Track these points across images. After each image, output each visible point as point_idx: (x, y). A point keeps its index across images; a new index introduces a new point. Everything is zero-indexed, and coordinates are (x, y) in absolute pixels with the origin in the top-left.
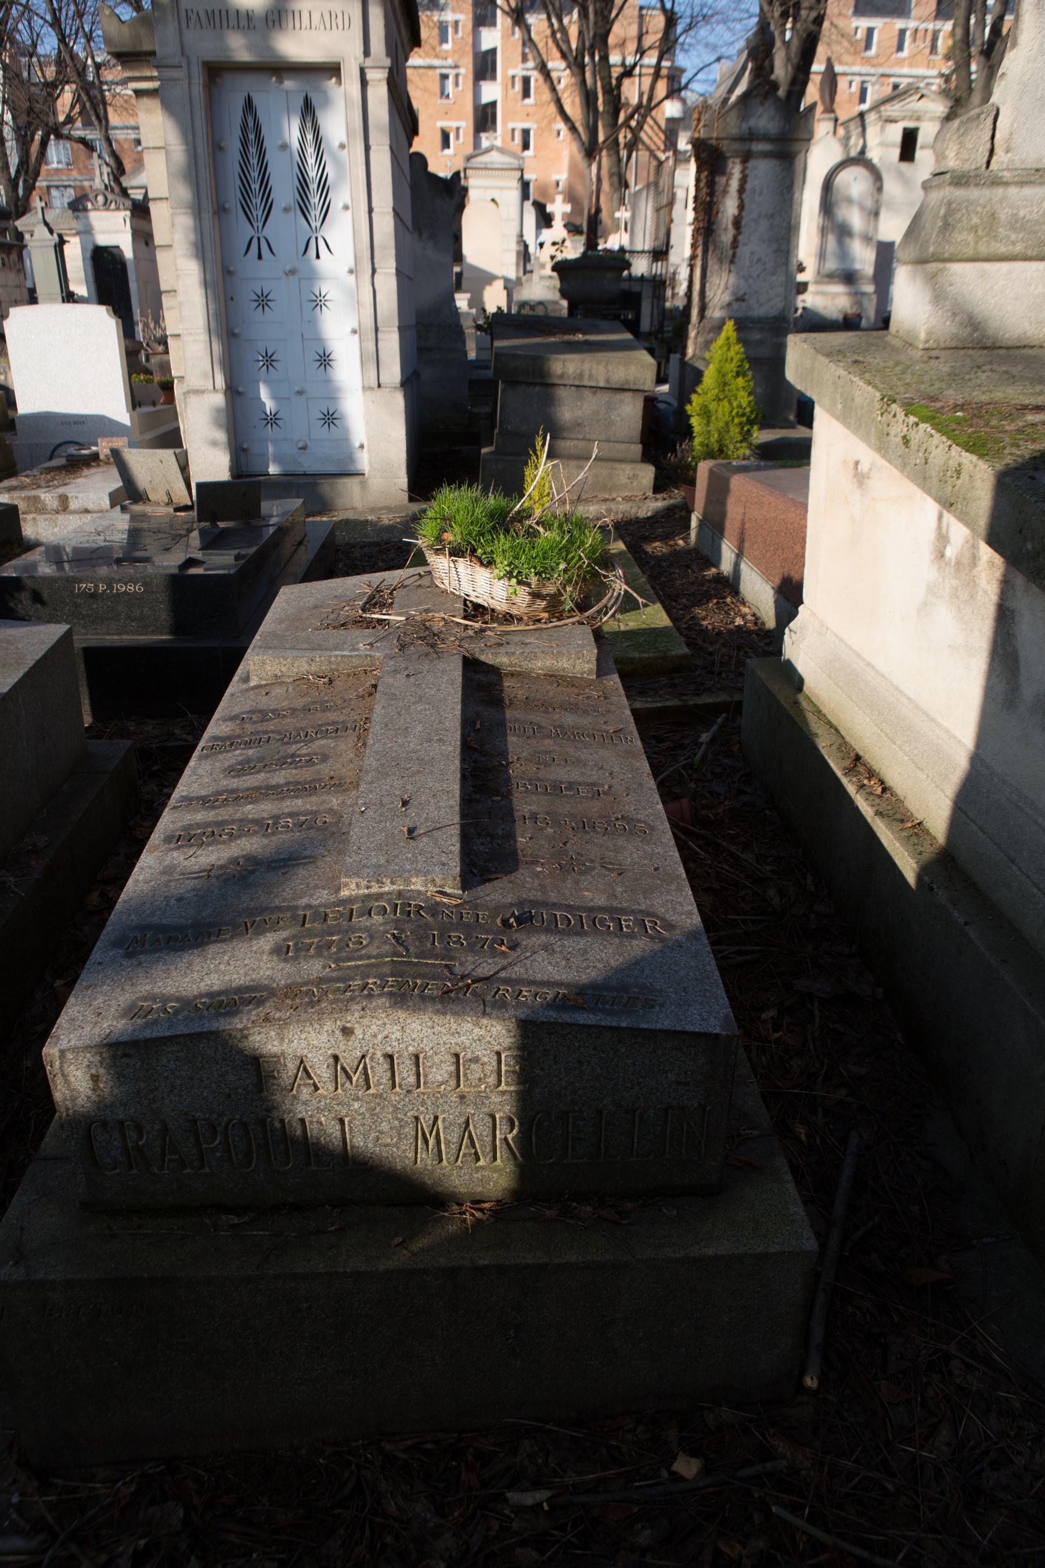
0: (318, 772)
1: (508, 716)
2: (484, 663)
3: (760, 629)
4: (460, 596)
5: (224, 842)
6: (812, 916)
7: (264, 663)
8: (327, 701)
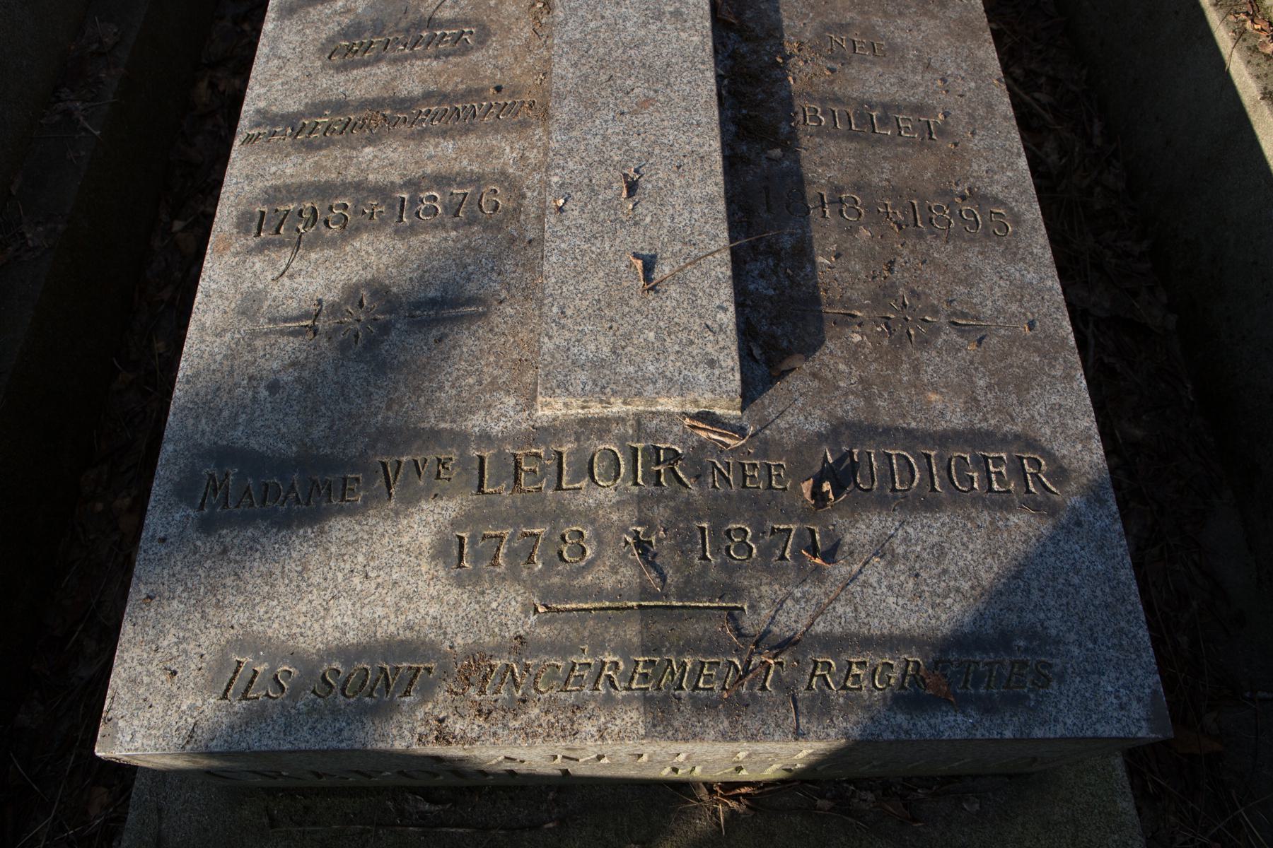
0: (474, 71)
5: (332, 243)
6: (1098, 189)
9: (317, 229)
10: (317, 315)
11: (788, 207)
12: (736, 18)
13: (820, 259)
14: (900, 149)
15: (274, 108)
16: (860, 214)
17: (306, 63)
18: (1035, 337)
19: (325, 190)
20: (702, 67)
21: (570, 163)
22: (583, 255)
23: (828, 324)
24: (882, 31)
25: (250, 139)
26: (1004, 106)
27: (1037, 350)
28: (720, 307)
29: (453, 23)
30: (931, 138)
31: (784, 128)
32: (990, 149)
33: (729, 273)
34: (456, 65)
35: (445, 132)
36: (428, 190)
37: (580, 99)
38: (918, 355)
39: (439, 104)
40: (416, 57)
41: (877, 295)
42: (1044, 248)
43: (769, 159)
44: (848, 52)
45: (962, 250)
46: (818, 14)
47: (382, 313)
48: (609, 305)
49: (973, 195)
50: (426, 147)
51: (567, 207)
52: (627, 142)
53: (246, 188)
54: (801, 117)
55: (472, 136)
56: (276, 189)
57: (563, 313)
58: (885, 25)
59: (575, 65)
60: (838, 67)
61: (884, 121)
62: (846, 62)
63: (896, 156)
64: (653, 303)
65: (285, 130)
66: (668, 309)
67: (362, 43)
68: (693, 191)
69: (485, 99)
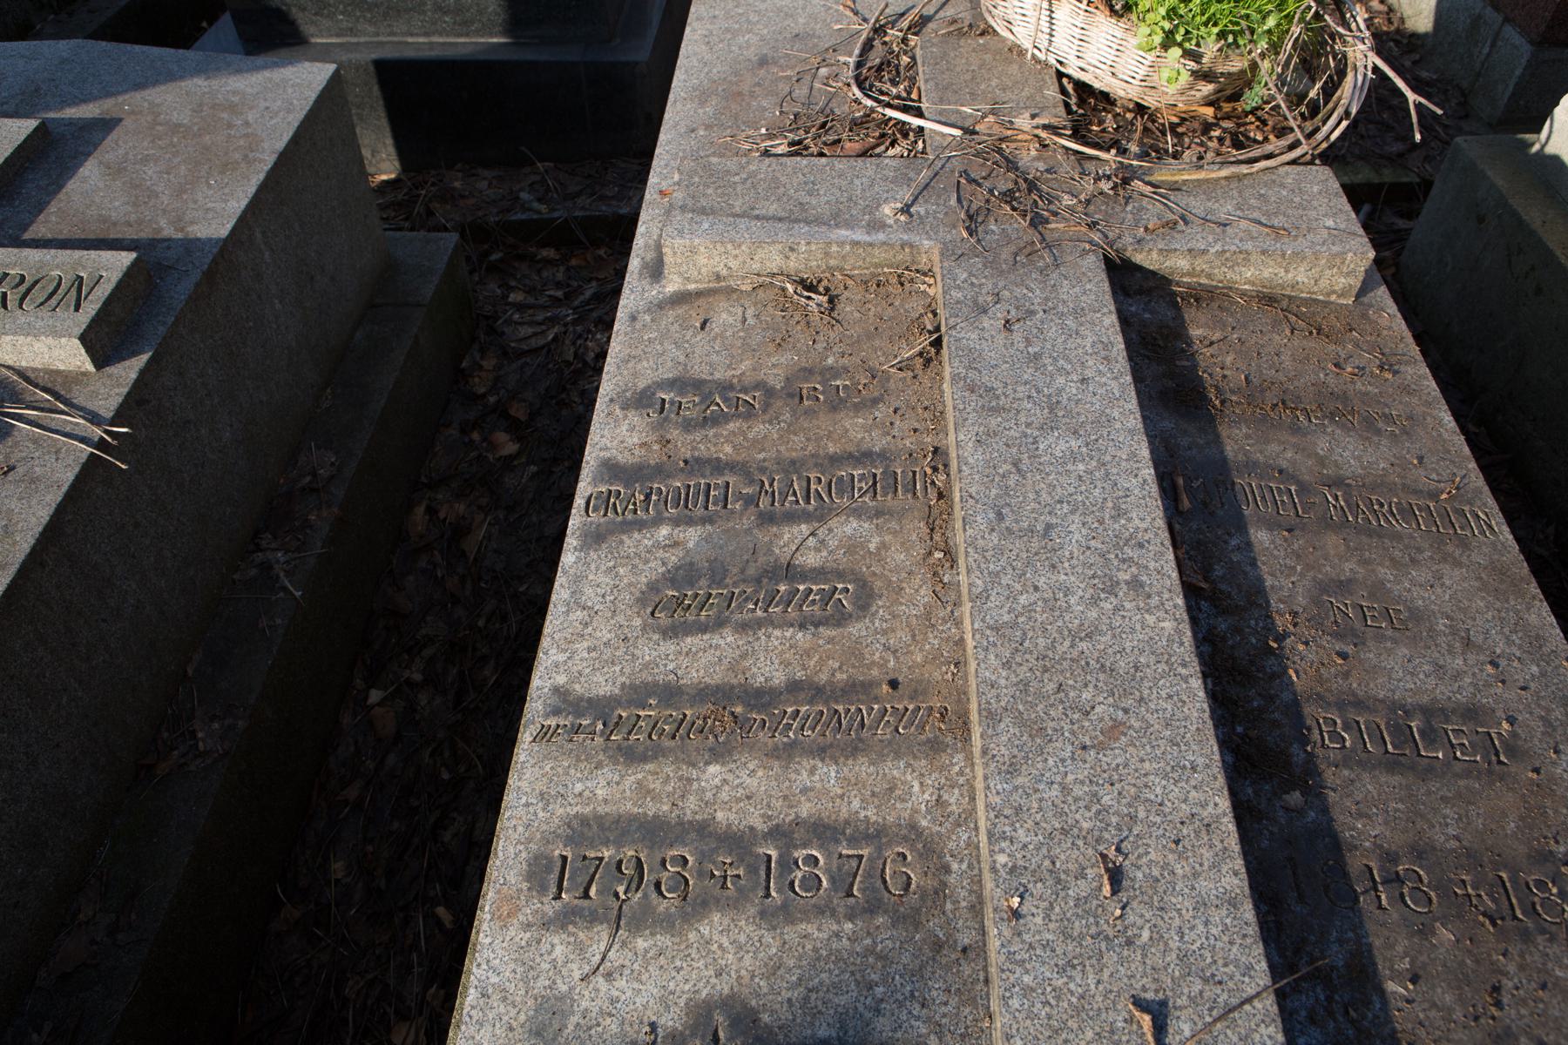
0: (855, 652)
1: (1230, 450)
2: (1139, 268)
3: (1398, 31)
4: (1047, 65)
5: (667, 924)
7: (693, 251)
8: (835, 372)
13: (1391, 986)
14: (1462, 783)
15: (577, 687)
16: (1430, 900)
17: (621, 619)
19: (654, 831)
20: (1183, 671)
21: (1020, 831)
24: (1397, 589)
29: (819, 574)
34: (831, 640)
36: (805, 846)
39: (811, 702)
43: (1287, 809)
44: (1358, 625)
46: (1308, 567)
50: (798, 772)
53: (541, 814)
56: (584, 821)
59: (1007, 665)
60: (1350, 649)
61: (1430, 735)
65: (593, 724)
68: (1203, 885)
69: (876, 699)
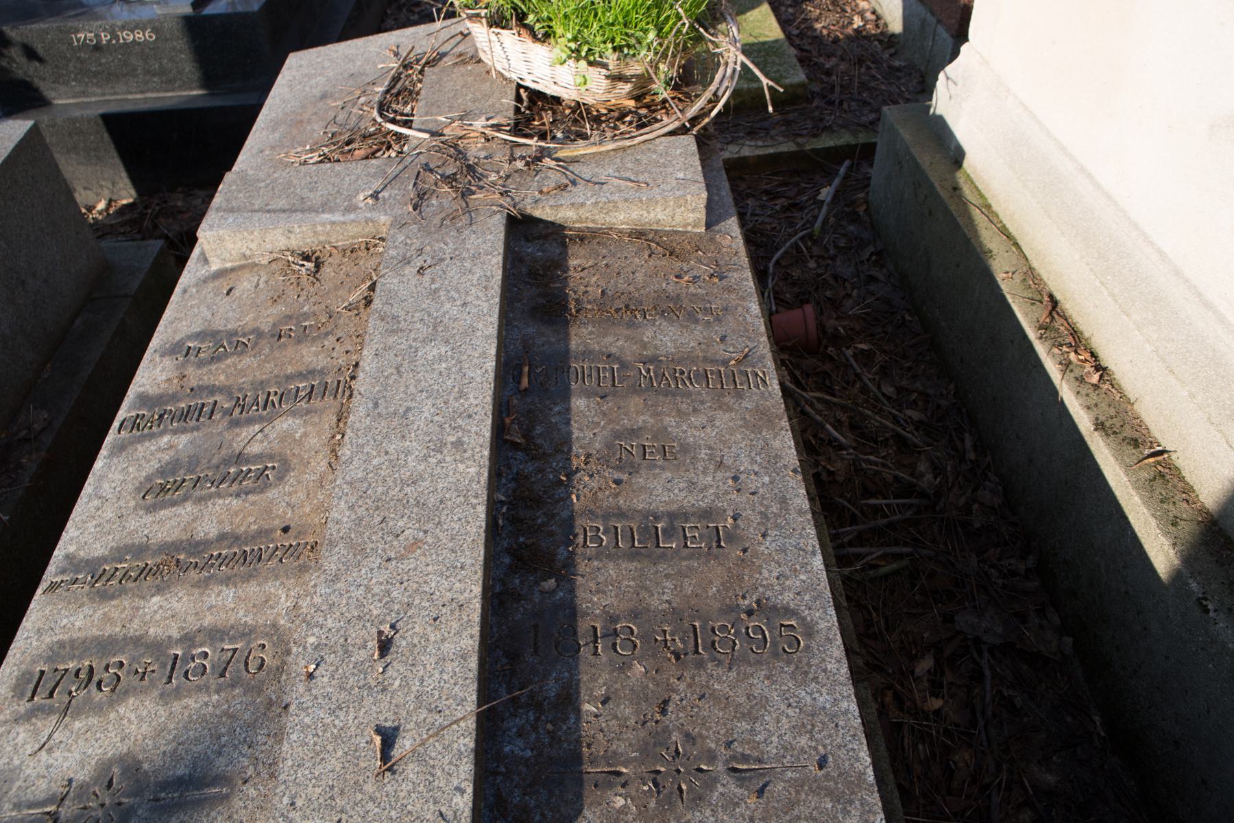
1: (574, 344)
2: (540, 221)
3: (882, 33)
4: (511, 81)
5: (98, 710)
6: (975, 507)
7: (222, 239)
8: (306, 316)
9: (89, 692)
10: (62, 800)
11: (556, 647)
12: (524, 437)
13: (587, 707)
14: (684, 563)
15: (82, 553)
16: (635, 646)
17: (122, 503)
18: (827, 776)
19: (105, 645)
20: (474, 501)
21: (329, 621)
22: (325, 731)
23: (588, 788)
24: (674, 431)
25: (53, 587)
26: (800, 498)
27: (830, 793)
28: (458, 789)
29: (259, 457)
30: (719, 546)
31: (562, 553)
32: (782, 550)
33: (472, 745)
34: (253, 503)
35: (229, 579)
36: (201, 646)
37: (351, 546)
38: (689, 817)
39: (230, 547)
40: (219, 496)
41: (647, 744)
42: (839, 661)
43: (542, 592)
44: (638, 459)
45: (746, 676)
46: (610, 421)
47: (128, 796)
48: (342, 792)
49: (762, 608)
50: (209, 596)
51: (317, 673)
52: (388, 593)
53: (35, 643)
54: (580, 539)
55: (253, 583)
56: (61, 644)
57: (292, 804)
58: (678, 425)
59: (351, 508)
60: (625, 477)
61: (669, 533)
62: (634, 470)
63: (680, 572)
64: (389, 788)
65: (86, 578)
66: (402, 794)
67: (175, 481)
68: (447, 646)
69: (272, 541)
